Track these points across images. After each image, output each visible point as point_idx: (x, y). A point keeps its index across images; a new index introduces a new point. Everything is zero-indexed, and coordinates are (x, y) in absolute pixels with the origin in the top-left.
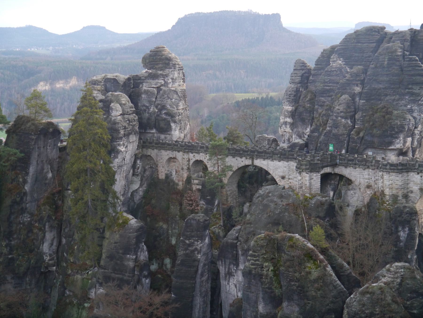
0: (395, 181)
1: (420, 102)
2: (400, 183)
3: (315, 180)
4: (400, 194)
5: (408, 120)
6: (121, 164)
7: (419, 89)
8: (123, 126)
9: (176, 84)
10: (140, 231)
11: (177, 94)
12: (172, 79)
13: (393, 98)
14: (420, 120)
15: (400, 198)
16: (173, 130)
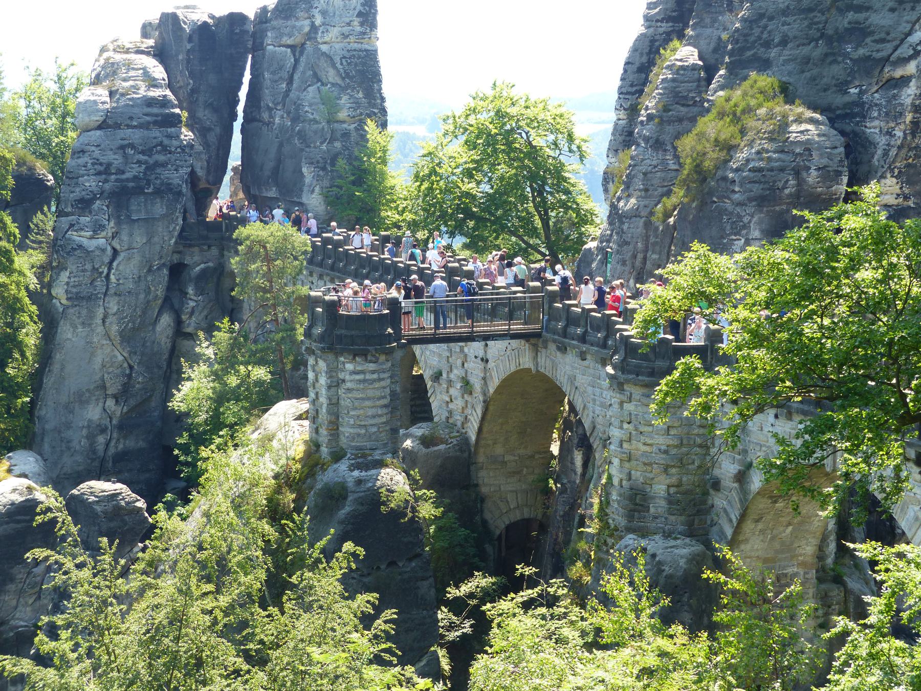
0: (642, 429)
1: (889, 72)
2: (662, 441)
3: (349, 390)
4: (660, 488)
5: (798, 150)
6: (85, 291)
7: (892, 10)
8: (97, 162)
9: (333, 33)
10: (18, 522)
11: (334, 65)
12: (324, 13)
13: (806, 50)
14: (886, 153)
15: (658, 506)
16: (305, 189)
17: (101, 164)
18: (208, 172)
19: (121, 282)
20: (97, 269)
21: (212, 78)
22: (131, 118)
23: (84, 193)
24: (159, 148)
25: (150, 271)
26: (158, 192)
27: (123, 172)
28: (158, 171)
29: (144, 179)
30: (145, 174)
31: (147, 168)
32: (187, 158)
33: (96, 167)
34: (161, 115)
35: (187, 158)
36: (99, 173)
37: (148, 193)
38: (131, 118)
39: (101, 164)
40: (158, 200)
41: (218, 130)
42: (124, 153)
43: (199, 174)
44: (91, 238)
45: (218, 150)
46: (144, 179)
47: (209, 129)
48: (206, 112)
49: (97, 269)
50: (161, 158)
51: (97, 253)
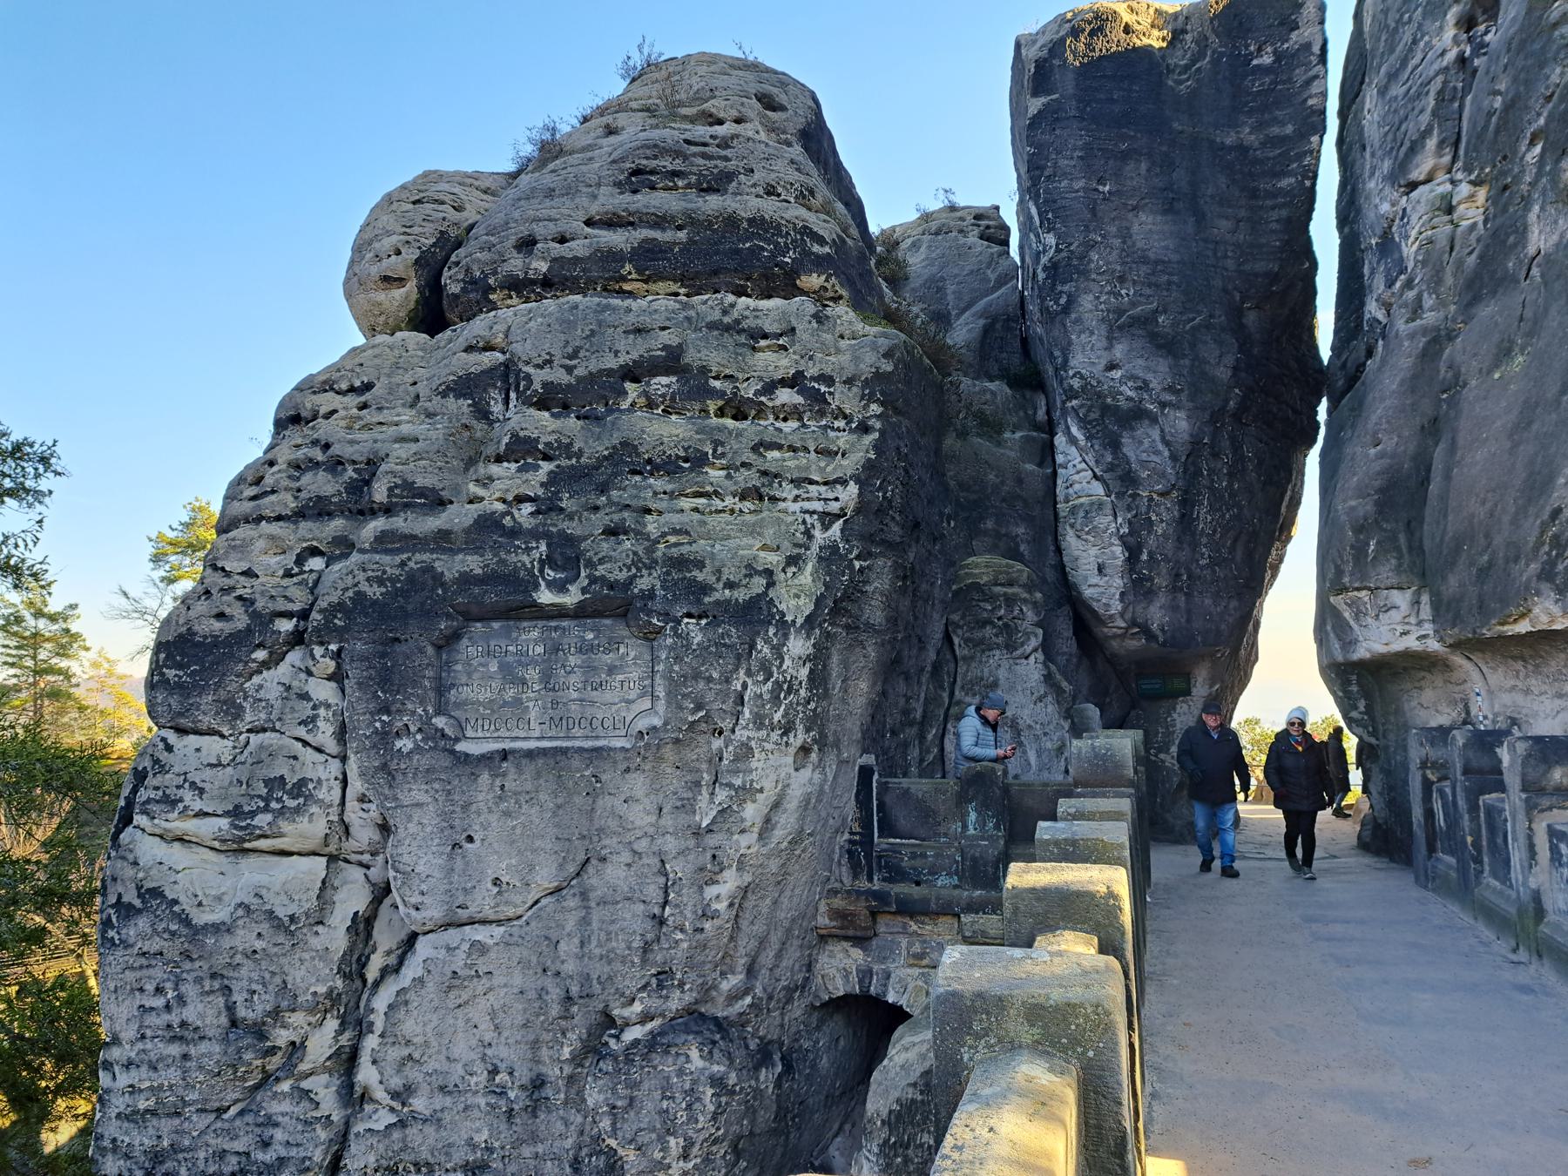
17: (336, 465)
18: (1138, 586)
19: (419, 1104)
20: (259, 1032)
21: (1150, 230)
22: (527, 244)
23: (201, 607)
24: (662, 383)
25: (592, 1049)
26: (614, 606)
27: (438, 502)
28: (632, 489)
29: (535, 534)
30: (547, 507)
31: (553, 479)
32: (843, 440)
33: (307, 478)
34: (690, 221)
35: (843, 440)
36: (318, 509)
37: (559, 612)
38: (527, 244)
39: (336, 465)
40: (632, 650)
41: (1180, 423)
42: (483, 413)
43: (1088, 592)
44: (237, 847)
45: (1186, 504)
46: (535, 534)
47: (1136, 415)
48: (1119, 351)
49: (259, 1032)
50: (669, 432)
51: (245, 938)
